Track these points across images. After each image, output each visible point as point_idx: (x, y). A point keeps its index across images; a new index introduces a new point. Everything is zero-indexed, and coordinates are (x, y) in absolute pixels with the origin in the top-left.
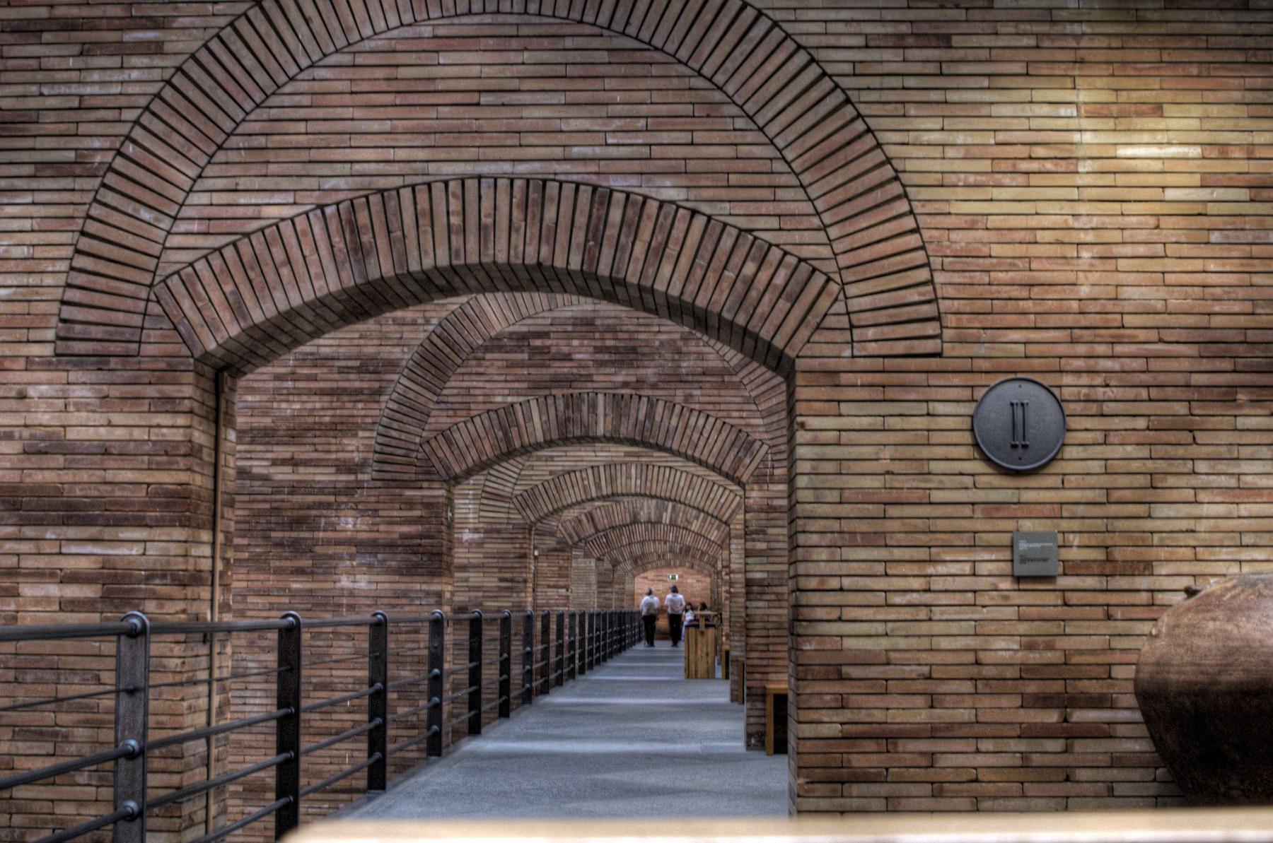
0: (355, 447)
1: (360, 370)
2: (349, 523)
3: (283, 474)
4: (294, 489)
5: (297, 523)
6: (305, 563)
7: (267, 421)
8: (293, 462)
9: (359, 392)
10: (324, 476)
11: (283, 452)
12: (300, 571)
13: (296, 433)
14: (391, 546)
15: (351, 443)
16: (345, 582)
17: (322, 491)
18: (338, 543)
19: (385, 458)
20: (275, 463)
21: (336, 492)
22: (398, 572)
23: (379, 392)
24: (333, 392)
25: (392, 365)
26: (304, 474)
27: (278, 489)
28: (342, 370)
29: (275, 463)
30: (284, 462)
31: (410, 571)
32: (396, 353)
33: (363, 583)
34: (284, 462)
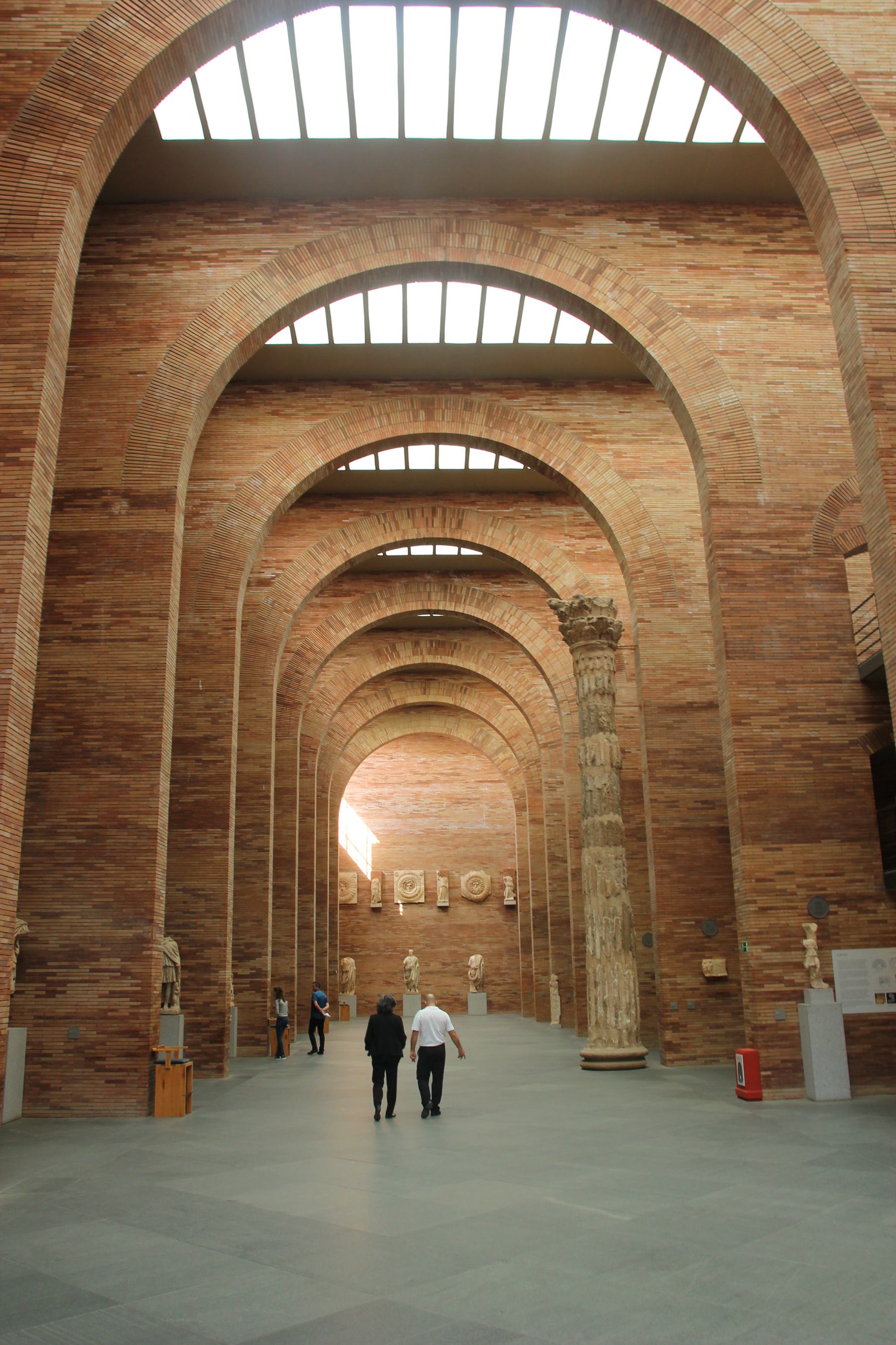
0: (806, 540)
1: (803, 509)
2: (807, 571)
3: (776, 551)
4: (782, 557)
5: (784, 572)
6: (790, 587)
7: (765, 530)
8: (779, 546)
9: (803, 518)
10: (793, 552)
11: (775, 542)
12: (788, 591)
13: (778, 534)
14: (825, 581)
15: (803, 539)
16: (808, 595)
17: (793, 558)
18: (803, 579)
19: (818, 543)
20: (772, 547)
21: (799, 558)
22: (830, 591)
23: (812, 518)
24: (791, 518)
25: (815, 508)
26: (784, 551)
27: (774, 557)
28: (795, 509)
29: (772, 547)
30: (775, 547)
31: (835, 590)
32: (816, 503)
33: (816, 596)
34: (775, 547)
